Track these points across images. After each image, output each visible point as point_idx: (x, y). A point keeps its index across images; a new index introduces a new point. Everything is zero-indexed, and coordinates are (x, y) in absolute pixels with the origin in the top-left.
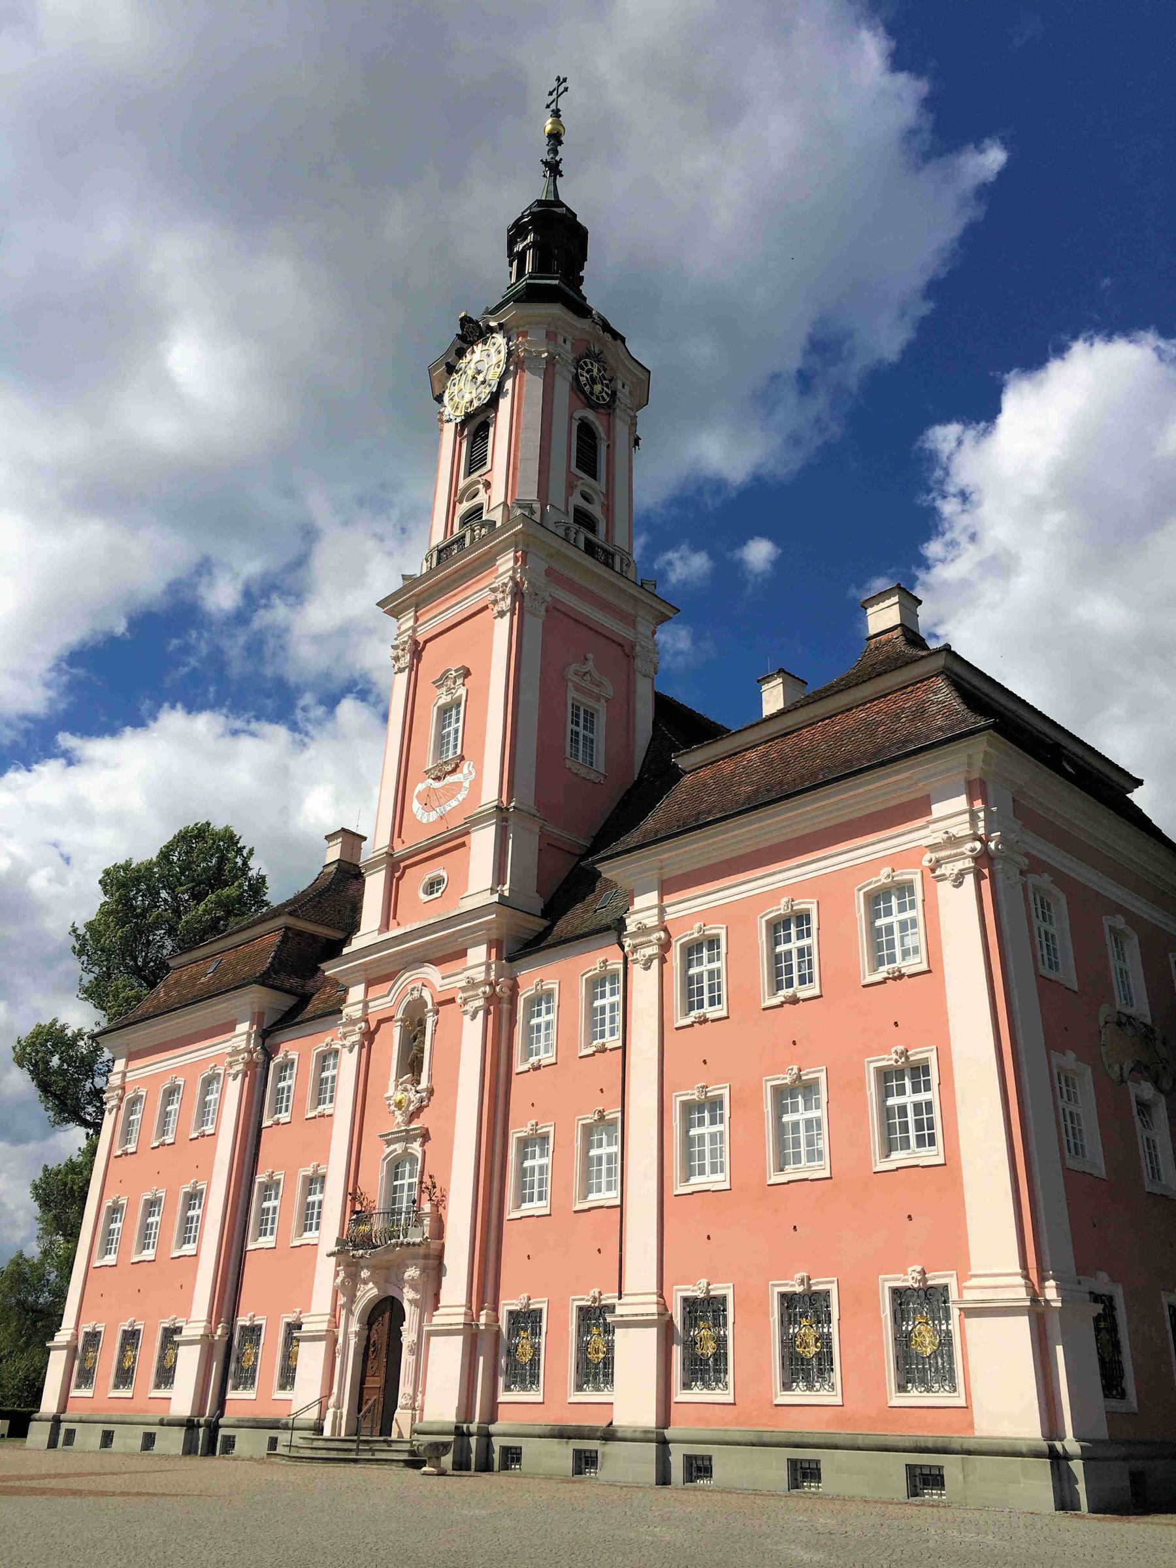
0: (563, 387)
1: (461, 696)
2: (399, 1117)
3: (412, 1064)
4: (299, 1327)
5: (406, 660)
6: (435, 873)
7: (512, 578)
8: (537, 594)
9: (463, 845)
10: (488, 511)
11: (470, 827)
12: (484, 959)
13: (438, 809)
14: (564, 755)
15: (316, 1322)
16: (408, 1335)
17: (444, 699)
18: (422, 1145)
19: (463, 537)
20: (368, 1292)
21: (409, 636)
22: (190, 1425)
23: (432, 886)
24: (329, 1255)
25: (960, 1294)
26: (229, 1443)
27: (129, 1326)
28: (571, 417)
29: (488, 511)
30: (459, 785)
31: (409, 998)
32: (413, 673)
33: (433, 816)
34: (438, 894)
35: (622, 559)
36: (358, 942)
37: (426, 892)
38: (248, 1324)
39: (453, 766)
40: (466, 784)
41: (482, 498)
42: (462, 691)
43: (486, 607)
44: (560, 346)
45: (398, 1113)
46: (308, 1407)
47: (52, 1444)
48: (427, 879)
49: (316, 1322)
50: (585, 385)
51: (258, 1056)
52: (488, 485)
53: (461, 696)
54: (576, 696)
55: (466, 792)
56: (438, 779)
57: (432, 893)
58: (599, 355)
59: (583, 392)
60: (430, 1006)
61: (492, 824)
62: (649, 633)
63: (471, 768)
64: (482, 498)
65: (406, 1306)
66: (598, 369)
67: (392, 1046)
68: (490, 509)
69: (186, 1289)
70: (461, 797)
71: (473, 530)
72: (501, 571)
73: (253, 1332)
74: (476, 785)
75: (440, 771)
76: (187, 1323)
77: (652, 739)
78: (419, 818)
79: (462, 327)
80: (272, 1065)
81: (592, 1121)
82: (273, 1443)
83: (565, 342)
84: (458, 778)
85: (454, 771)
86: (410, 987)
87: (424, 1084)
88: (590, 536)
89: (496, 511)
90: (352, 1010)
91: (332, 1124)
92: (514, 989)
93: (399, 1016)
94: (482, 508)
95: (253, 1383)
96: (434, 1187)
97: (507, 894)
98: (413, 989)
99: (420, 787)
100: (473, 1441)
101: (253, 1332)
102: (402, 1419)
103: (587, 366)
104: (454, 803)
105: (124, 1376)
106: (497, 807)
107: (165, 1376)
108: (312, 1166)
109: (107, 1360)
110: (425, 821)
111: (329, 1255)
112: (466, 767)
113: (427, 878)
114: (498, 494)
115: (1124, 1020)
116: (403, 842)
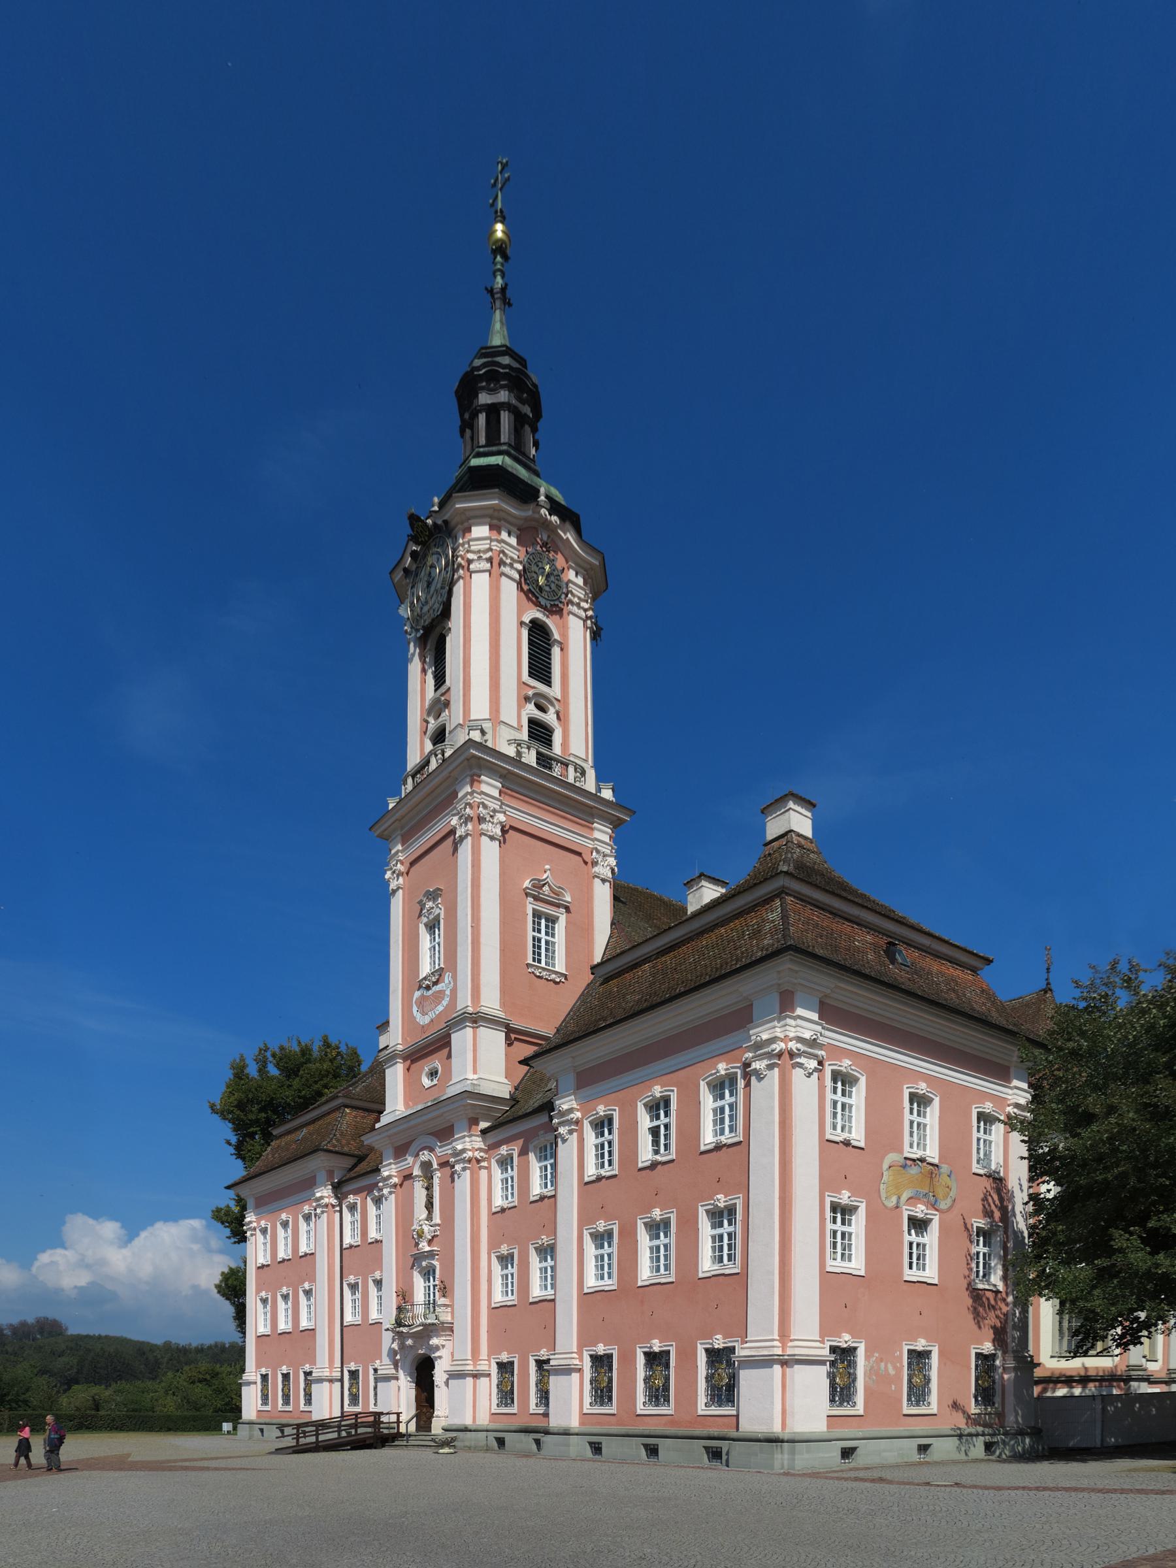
0: (509, 590)
1: (439, 914)
6: (432, 1066)
11: (450, 1029)
30: (442, 992)
34: (435, 1082)
40: (448, 992)
53: (439, 914)
57: (432, 1080)
60: (435, 1166)
70: (445, 1003)
74: (454, 991)
75: (429, 980)
78: (418, 1020)
85: (436, 983)
87: (437, 1219)
96: (445, 1288)
112: (447, 977)
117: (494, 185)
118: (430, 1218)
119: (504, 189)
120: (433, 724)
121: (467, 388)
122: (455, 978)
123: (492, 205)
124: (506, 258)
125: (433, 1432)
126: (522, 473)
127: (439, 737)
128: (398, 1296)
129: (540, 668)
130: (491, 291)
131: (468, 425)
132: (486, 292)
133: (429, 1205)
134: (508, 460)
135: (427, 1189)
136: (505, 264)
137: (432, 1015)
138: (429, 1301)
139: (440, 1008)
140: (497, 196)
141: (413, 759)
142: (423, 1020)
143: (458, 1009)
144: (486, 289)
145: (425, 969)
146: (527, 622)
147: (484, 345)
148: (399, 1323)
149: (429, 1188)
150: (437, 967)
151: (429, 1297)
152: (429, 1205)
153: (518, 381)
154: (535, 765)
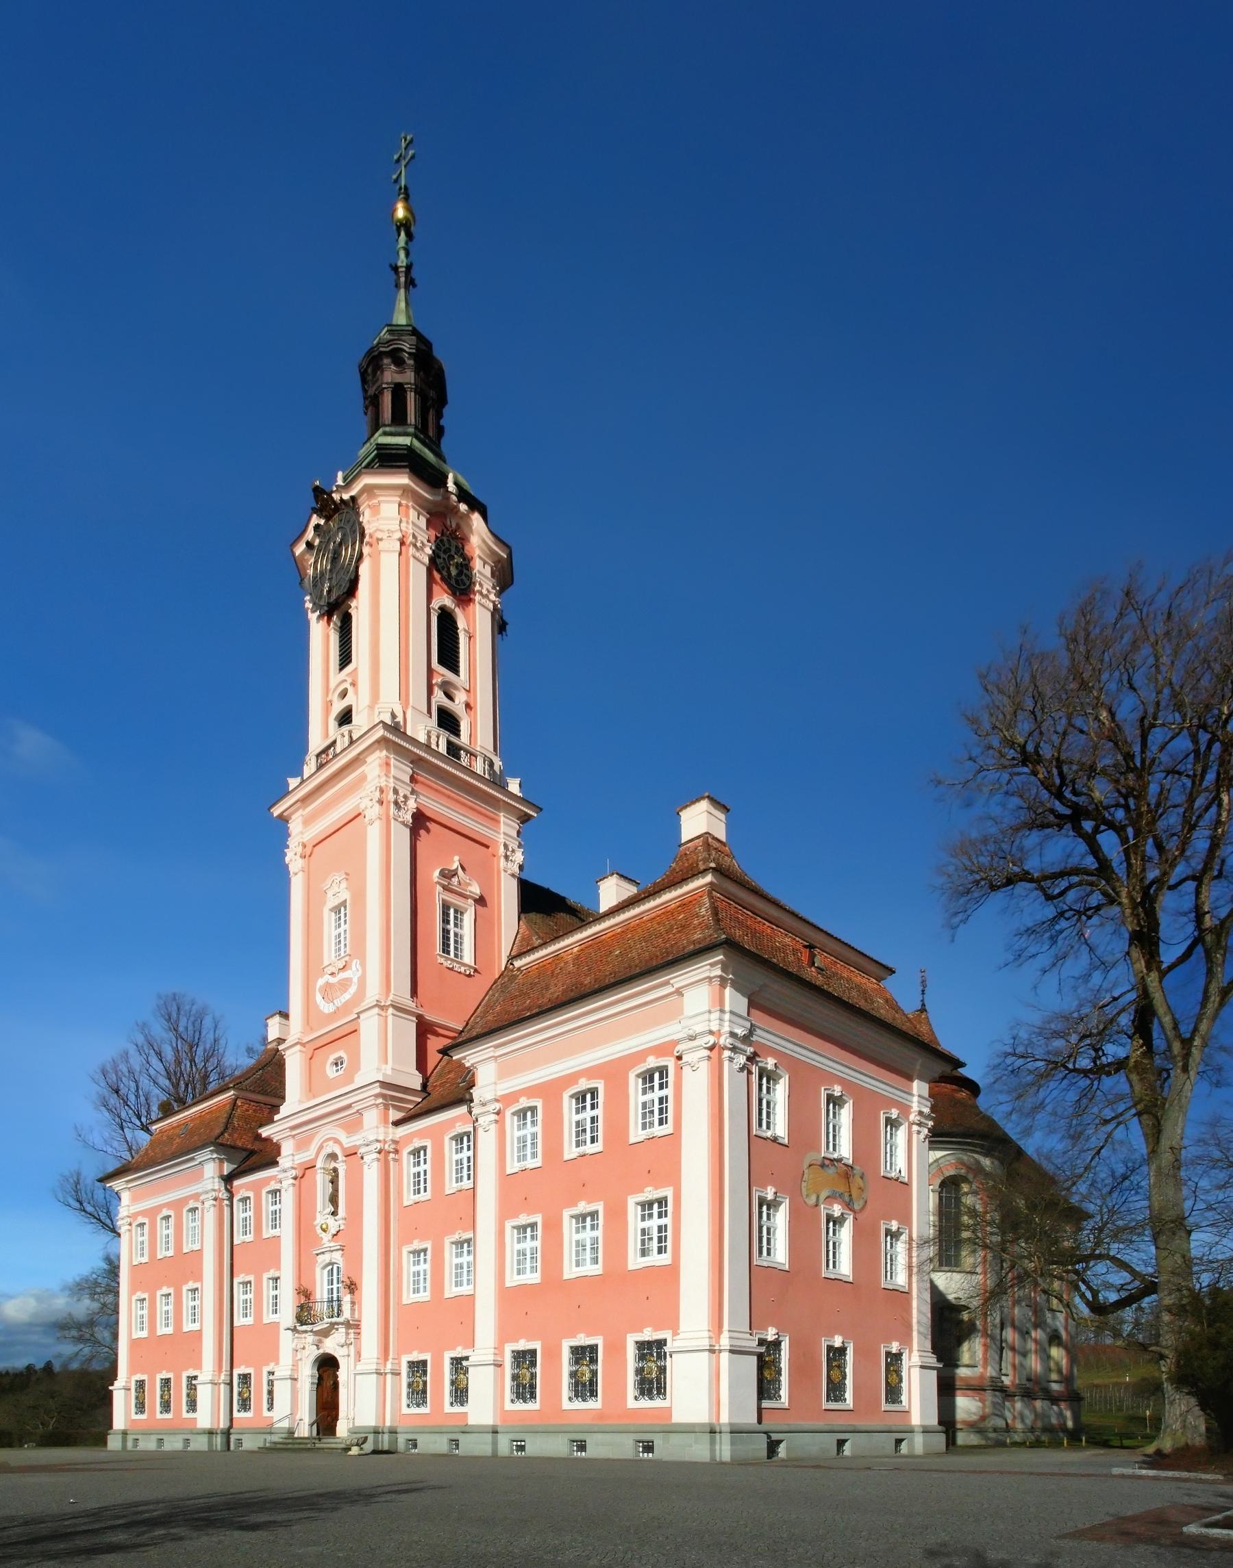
2: (326, 1238)
4: (273, 1373)
9: (356, 1031)
30: (349, 980)
34: (341, 1072)
36: (285, 1110)
39: (344, 963)
40: (355, 980)
52: (354, 684)
56: (332, 974)
57: (337, 1071)
65: (342, 1362)
68: (360, 710)
70: (353, 989)
90: (284, 1161)
97: (389, 1072)
99: (321, 982)
100: (386, 1437)
102: (342, 1429)
105: (166, 1406)
107: (192, 1405)
109: (154, 1396)
110: (326, 1011)
112: (355, 964)
113: (332, 1058)
115: (827, 1162)
117: (398, 161)
118: (334, 1214)
119: (408, 167)
120: (338, 707)
121: (372, 363)
122: (363, 965)
123: (397, 181)
124: (410, 236)
125: (338, 1434)
126: (430, 456)
127: (345, 718)
128: (299, 1293)
129: (449, 656)
130: (395, 269)
131: (373, 402)
132: (390, 269)
133: (334, 1200)
134: (417, 444)
135: (332, 1182)
136: (410, 243)
137: (339, 1002)
138: (332, 1297)
139: (347, 996)
140: (401, 173)
141: (316, 742)
142: (327, 1008)
144: (391, 266)
145: (329, 955)
146: (437, 608)
147: (389, 323)
148: (301, 1320)
149: (334, 1181)
150: (343, 955)
151: (332, 1294)
152: (334, 1200)
153: (425, 360)
154: (445, 754)
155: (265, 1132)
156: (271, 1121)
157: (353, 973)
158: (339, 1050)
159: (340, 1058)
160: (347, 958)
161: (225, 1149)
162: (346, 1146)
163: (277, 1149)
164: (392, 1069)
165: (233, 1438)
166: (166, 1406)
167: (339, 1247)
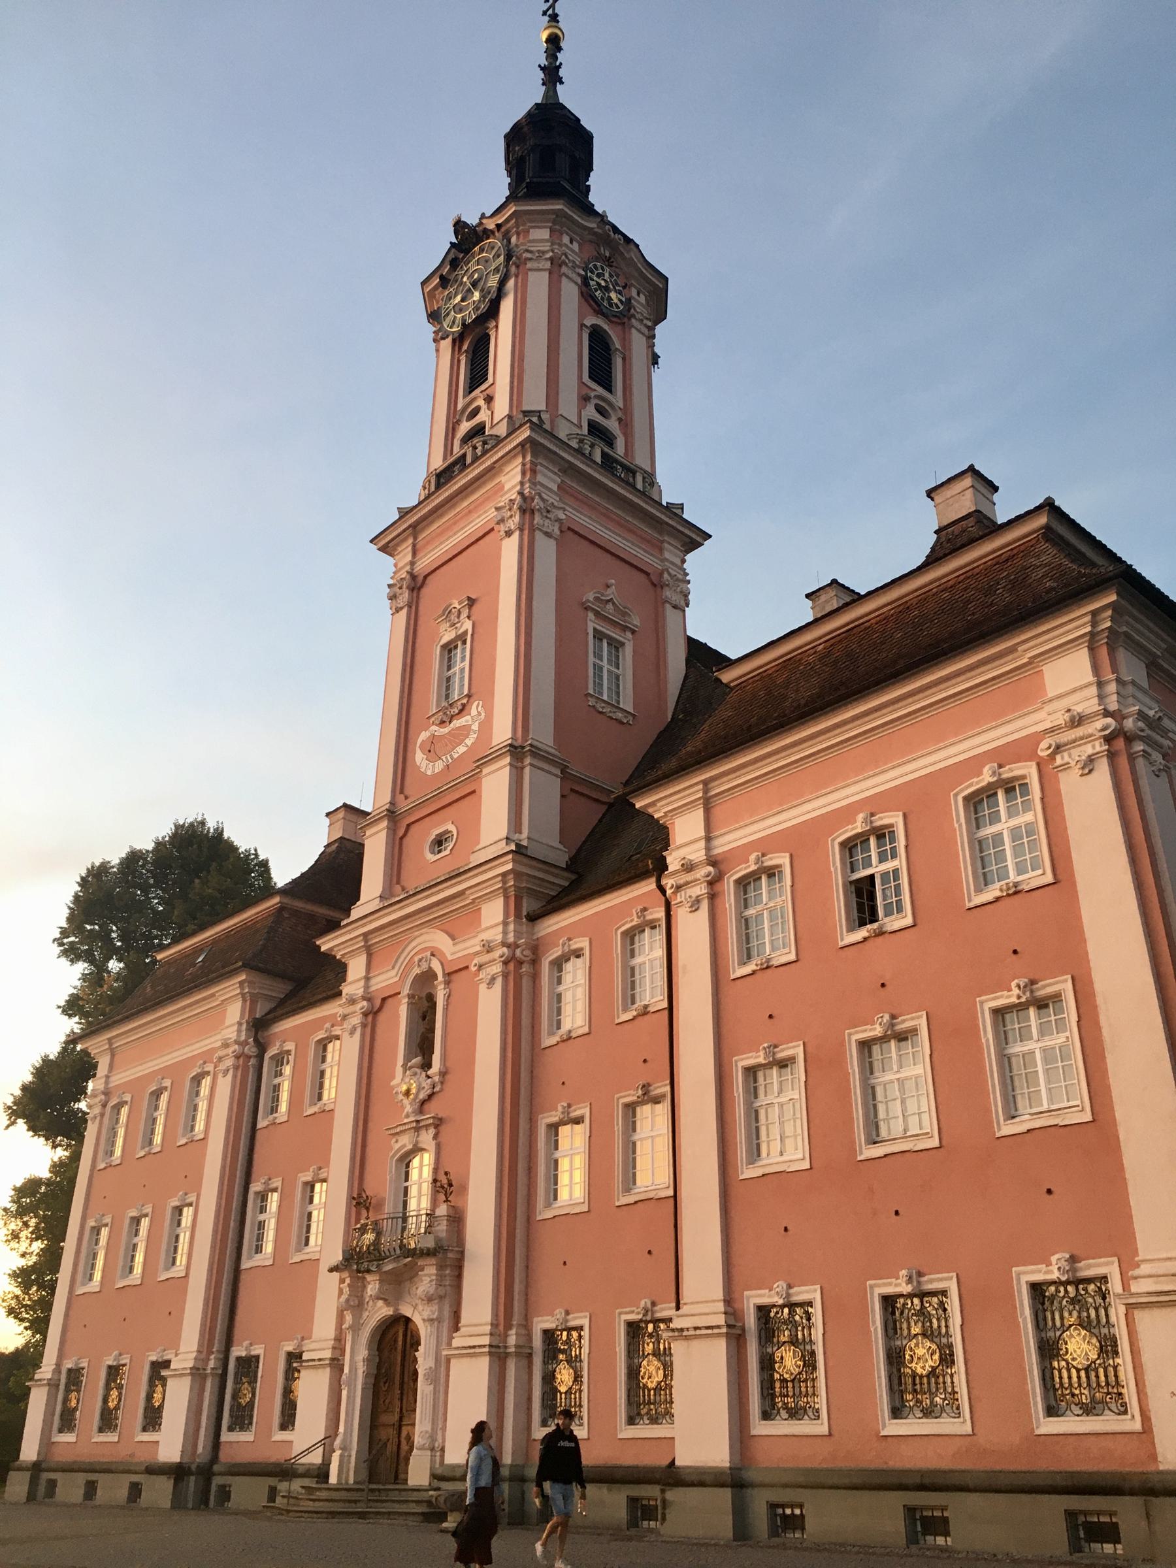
0: (570, 291)
1: (466, 632)
3: (422, 1046)
5: (405, 596)
7: (521, 493)
8: (548, 511)
10: (492, 427)
12: (500, 918)
13: (444, 758)
14: (587, 688)
15: (319, 1347)
16: (424, 1360)
17: (448, 637)
18: (435, 1137)
19: (464, 455)
20: (382, 1311)
21: (408, 572)
22: (178, 1472)
23: (439, 842)
24: (331, 1270)
25: (1125, 1286)
26: (225, 1494)
27: (115, 1360)
28: (582, 326)
29: (492, 427)
30: (467, 729)
31: (417, 971)
32: (414, 607)
33: (439, 766)
34: (448, 852)
35: (644, 478)
37: (433, 852)
38: (243, 1354)
39: (460, 708)
40: (475, 727)
41: (483, 416)
42: (468, 625)
43: (492, 529)
44: (566, 245)
45: (406, 1102)
46: (308, 1451)
47: (31, 1497)
48: (433, 837)
49: (319, 1347)
50: (596, 290)
51: (250, 1049)
52: (489, 399)
53: (466, 632)
54: (598, 627)
55: (475, 736)
57: (440, 852)
58: (610, 258)
59: (594, 298)
60: (440, 978)
61: (505, 766)
62: (678, 562)
63: (479, 709)
64: (483, 416)
66: (610, 273)
67: (398, 1028)
69: (175, 1315)
70: (469, 742)
71: (475, 448)
72: (507, 487)
73: (248, 1365)
74: (487, 725)
76: (176, 1355)
77: (686, 677)
79: (456, 233)
80: (267, 1056)
81: (635, 1098)
82: (273, 1493)
83: (571, 242)
84: (467, 721)
86: (416, 959)
88: (606, 450)
89: (500, 424)
90: (353, 986)
91: (332, 1118)
92: (536, 951)
93: (406, 991)
94: (484, 427)
95: (251, 1423)
96: (451, 1185)
98: (420, 960)
101: (248, 1365)
103: (597, 269)
104: (461, 749)
106: (510, 745)
107: (153, 1418)
108: (311, 1170)
110: (429, 773)
111: (331, 1270)
114: (502, 407)
116: (406, 798)
118: (427, 1065)
139: (461, 749)
143: (493, 745)
155: (326, 944)
156: (333, 926)
157: (471, 719)
158: (444, 822)
159: (447, 832)
160: (465, 701)
161: (258, 964)
162: (450, 958)
163: (339, 969)
164: (529, 838)
165: (217, 1481)
166: (108, 1421)
167: (431, 1121)
